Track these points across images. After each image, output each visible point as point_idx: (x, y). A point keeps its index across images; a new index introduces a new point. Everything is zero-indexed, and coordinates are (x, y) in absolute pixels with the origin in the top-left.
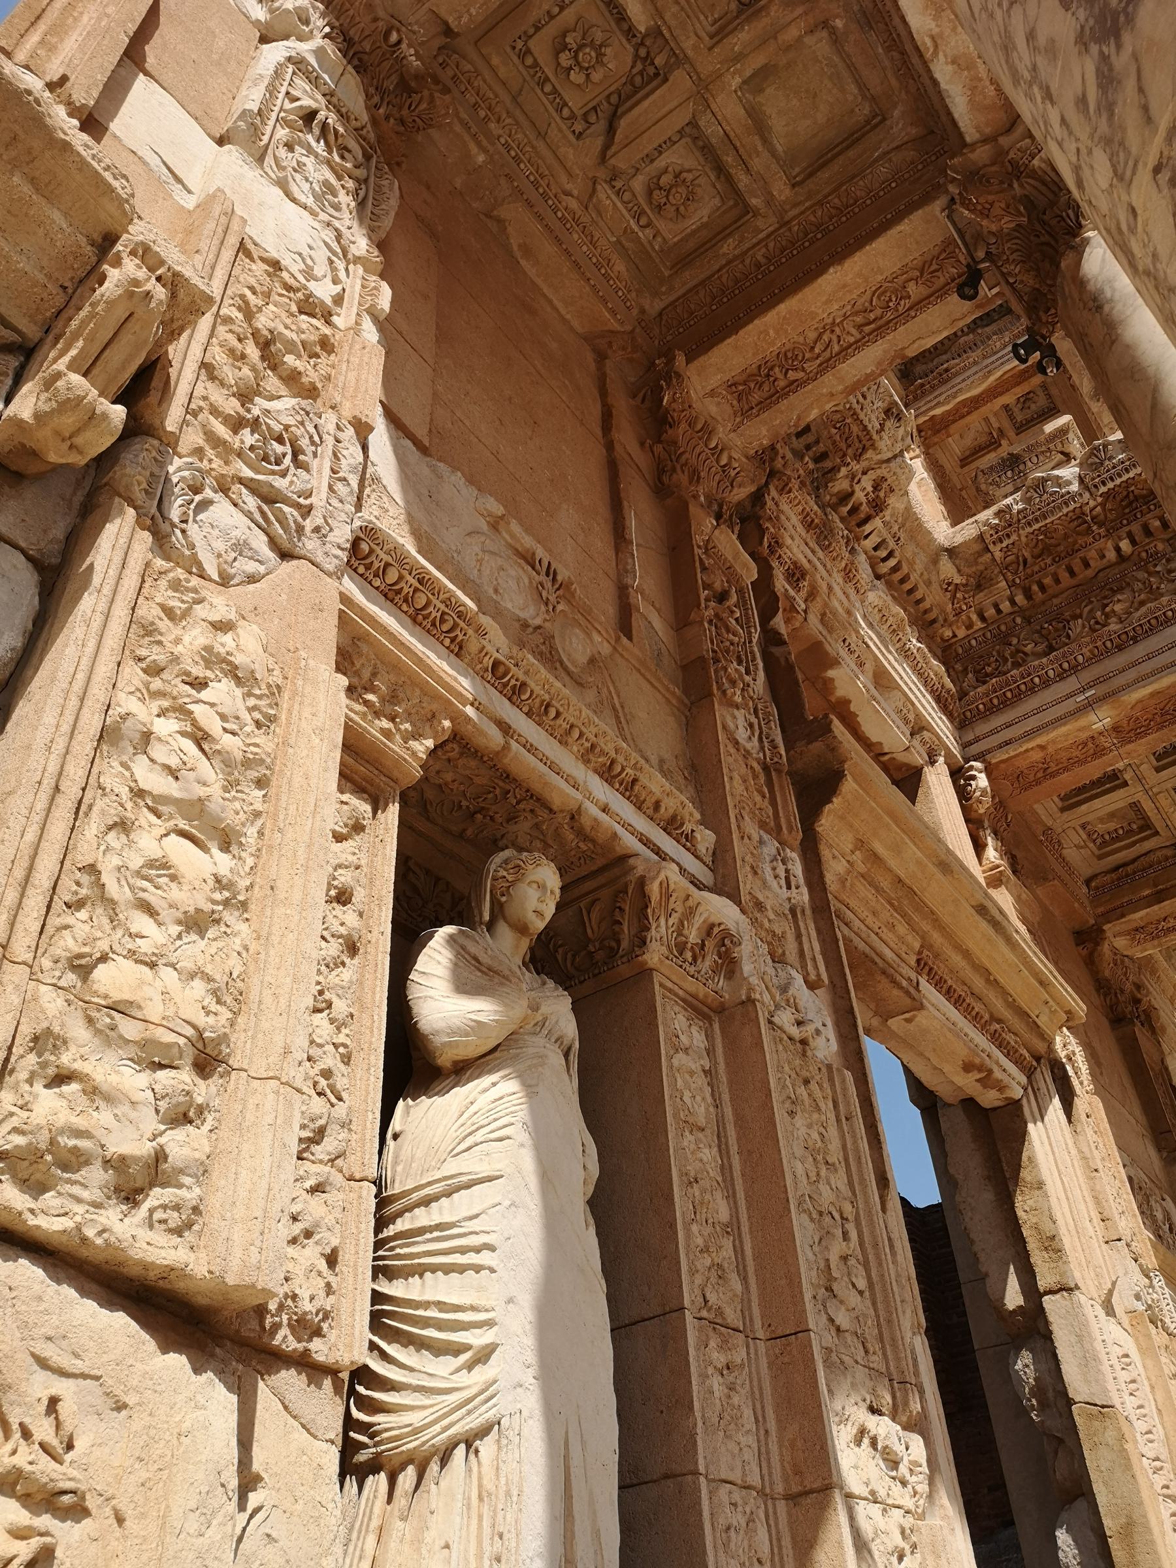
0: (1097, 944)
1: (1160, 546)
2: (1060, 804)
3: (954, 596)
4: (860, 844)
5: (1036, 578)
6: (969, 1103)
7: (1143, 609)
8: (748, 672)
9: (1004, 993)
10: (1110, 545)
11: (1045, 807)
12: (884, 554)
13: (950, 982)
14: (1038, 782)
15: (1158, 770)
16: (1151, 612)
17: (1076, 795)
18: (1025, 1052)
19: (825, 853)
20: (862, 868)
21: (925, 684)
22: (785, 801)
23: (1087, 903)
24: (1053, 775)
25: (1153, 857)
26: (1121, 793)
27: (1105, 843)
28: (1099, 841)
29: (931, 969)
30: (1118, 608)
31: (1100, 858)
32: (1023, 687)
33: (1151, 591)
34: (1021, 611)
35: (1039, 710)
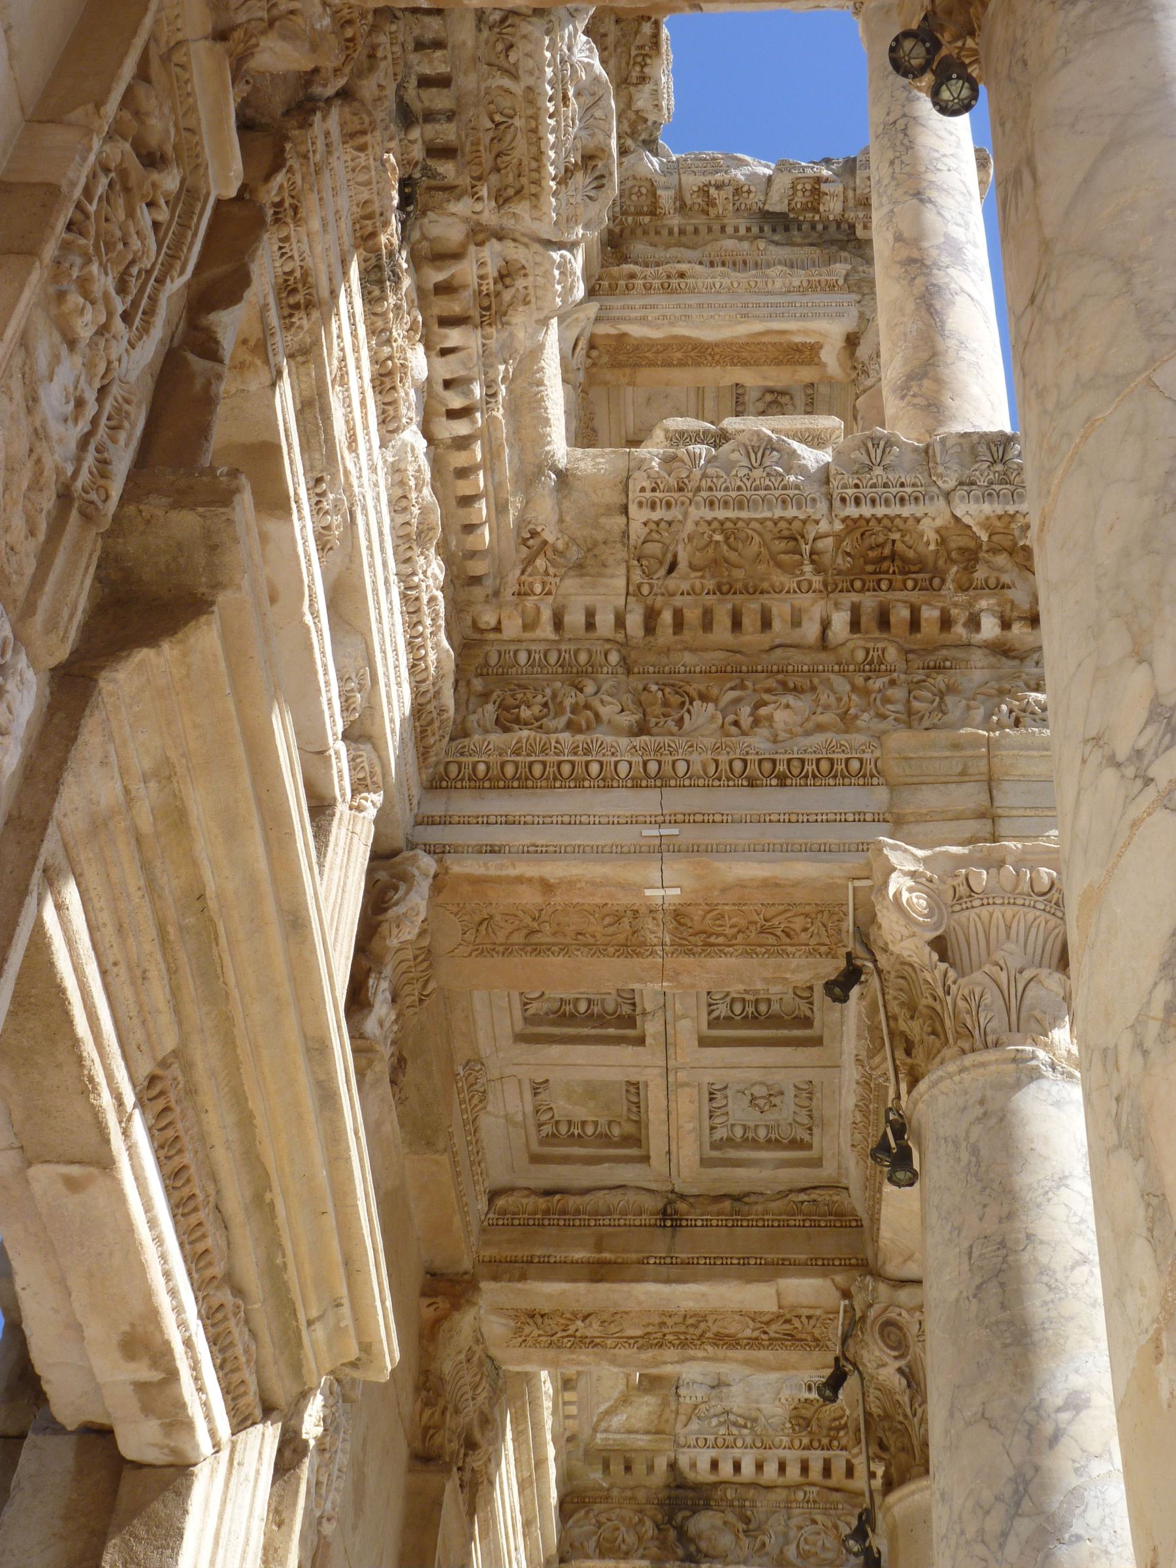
0: (456, 1307)
1: (892, 654)
2: (519, 1026)
3: (530, 561)
4: (164, 773)
5: (678, 601)
6: (99, 1435)
7: (819, 739)
8: (126, 317)
9: (272, 1243)
11: (490, 1015)
12: (457, 403)
15: (704, 1042)
17: (553, 1023)
19: (91, 737)
20: (145, 822)
21: (412, 667)
23: (475, 1228)
24: (538, 950)
25: (616, 1200)
26: (626, 1053)
28: (547, 1129)
29: (167, 1109)
30: (780, 716)
31: (535, 1159)
32: (566, 769)
33: (844, 716)
34: (624, 645)
35: (573, 821)
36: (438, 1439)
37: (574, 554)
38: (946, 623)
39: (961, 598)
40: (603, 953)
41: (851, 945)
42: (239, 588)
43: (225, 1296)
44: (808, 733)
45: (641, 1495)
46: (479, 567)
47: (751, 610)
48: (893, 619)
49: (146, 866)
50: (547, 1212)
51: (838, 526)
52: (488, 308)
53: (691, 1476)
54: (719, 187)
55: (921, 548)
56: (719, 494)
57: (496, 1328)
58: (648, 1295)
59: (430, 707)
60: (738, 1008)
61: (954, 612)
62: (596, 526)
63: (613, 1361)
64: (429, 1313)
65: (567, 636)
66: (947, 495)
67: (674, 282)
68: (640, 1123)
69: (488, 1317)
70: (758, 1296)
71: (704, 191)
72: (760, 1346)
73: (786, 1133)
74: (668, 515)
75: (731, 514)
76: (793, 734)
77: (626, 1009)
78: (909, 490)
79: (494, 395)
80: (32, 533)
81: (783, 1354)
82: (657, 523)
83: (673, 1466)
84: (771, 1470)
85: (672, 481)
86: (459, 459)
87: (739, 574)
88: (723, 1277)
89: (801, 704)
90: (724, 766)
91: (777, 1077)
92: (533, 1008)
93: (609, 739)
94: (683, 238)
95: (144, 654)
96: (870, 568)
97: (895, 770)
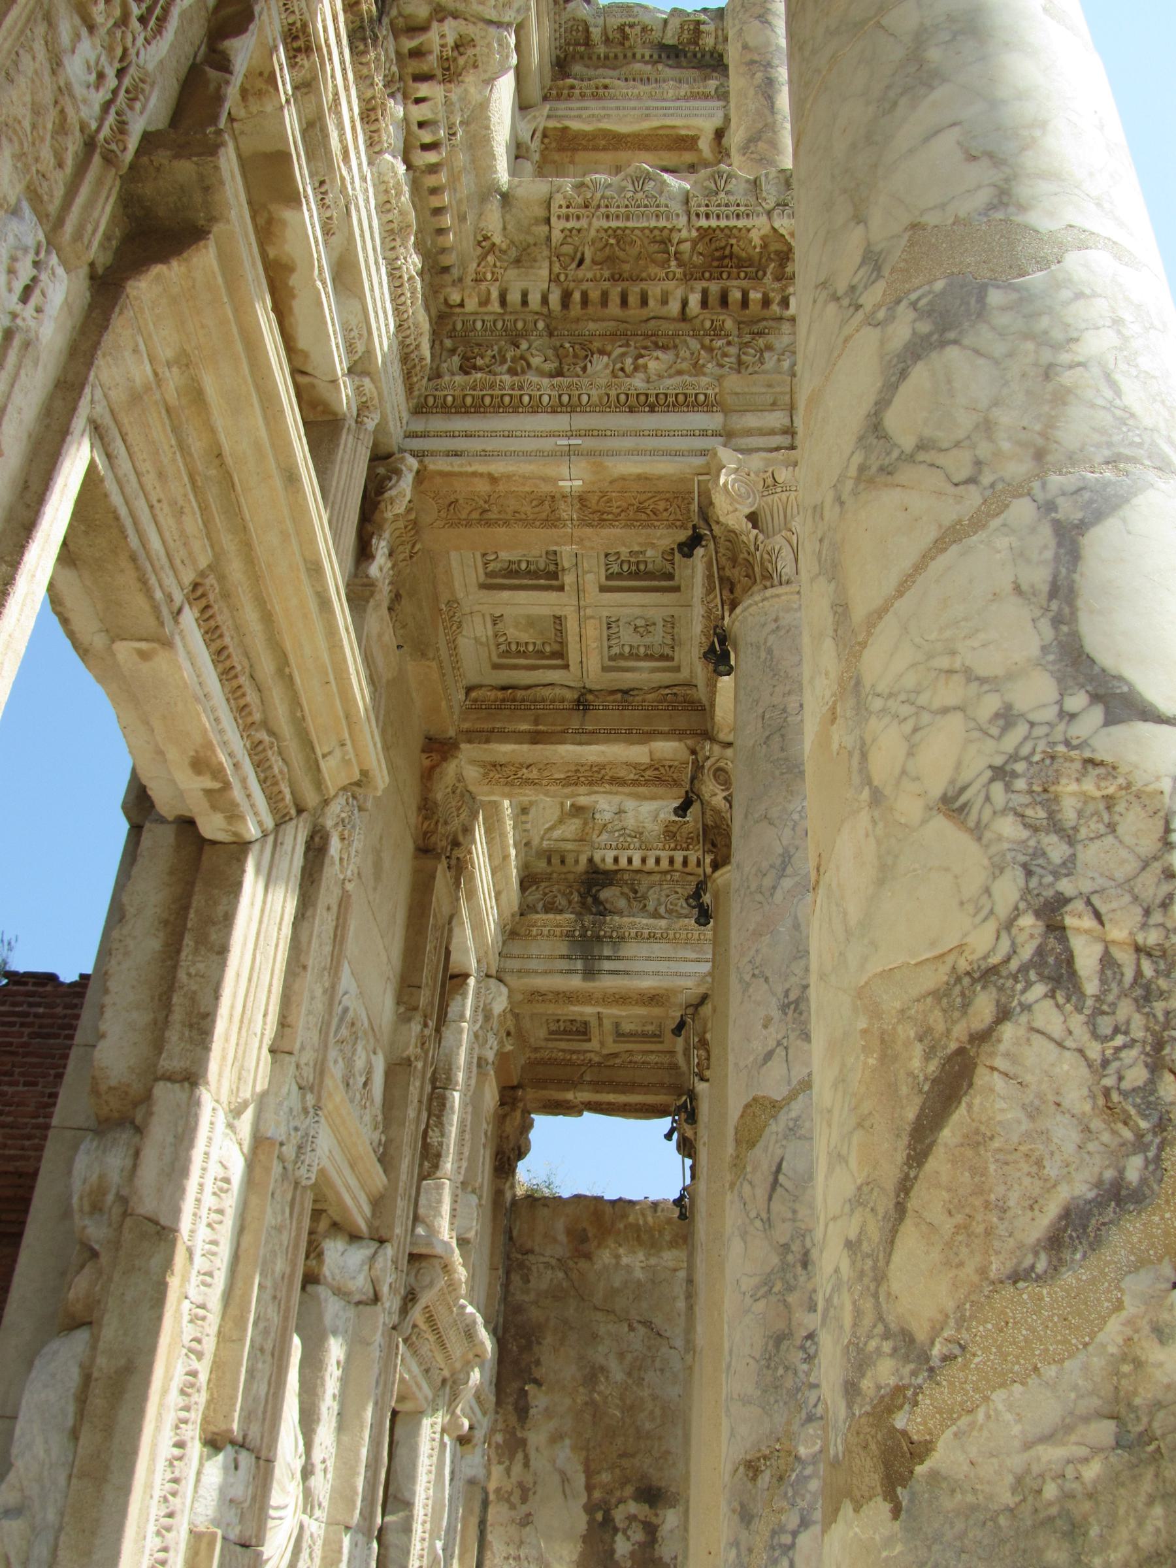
0: (444, 759)
1: (729, 324)
2: (482, 578)
3: (483, 257)
4: (184, 361)
5: (585, 286)
8: (143, 20)
9: (295, 702)
10: (679, 293)
11: (462, 569)
12: (427, 138)
13: (227, 640)
14: (469, 524)
15: (603, 589)
16: (685, 385)
17: (504, 577)
18: (287, 792)
19: (121, 329)
20: (172, 396)
22: (90, 205)
23: (457, 710)
24: (488, 523)
25: (547, 692)
26: (552, 596)
27: (507, 653)
28: (503, 647)
29: (207, 607)
31: (496, 667)
32: (507, 400)
34: (549, 315)
36: (433, 839)
37: (513, 253)
38: (766, 302)
39: (777, 285)
40: (532, 525)
41: (696, 519)
42: (228, 221)
43: (263, 735)
44: (670, 377)
45: (571, 877)
46: (446, 260)
47: (635, 291)
48: (730, 300)
49: (176, 430)
50: (503, 700)
51: (694, 234)
52: (448, 69)
53: (602, 866)
54: (632, 26)
55: (750, 251)
56: (613, 210)
57: (472, 773)
58: (567, 751)
59: (413, 356)
60: (625, 567)
61: (772, 295)
62: (528, 232)
63: (546, 794)
64: (427, 763)
65: (509, 309)
66: (769, 213)
67: (601, 91)
68: (563, 643)
69: (466, 765)
70: (638, 753)
71: (621, 29)
72: (640, 785)
73: (657, 650)
74: (578, 225)
75: (620, 224)
76: (660, 377)
77: (552, 568)
78: (742, 209)
79: (454, 134)
80: (60, 165)
81: (654, 789)
82: (571, 231)
83: (591, 860)
84: (651, 862)
85: (580, 200)
86: (430, 181)
87: (626, 267)
88: (615, 741)
89: (666, 357)
90: (613, 399)
91: (652, 613)
92: (491, 567)
93: (535, 379)
94: (608, 62)
95: (158, 269)
96: (715, 264)
97: (729, 400)
